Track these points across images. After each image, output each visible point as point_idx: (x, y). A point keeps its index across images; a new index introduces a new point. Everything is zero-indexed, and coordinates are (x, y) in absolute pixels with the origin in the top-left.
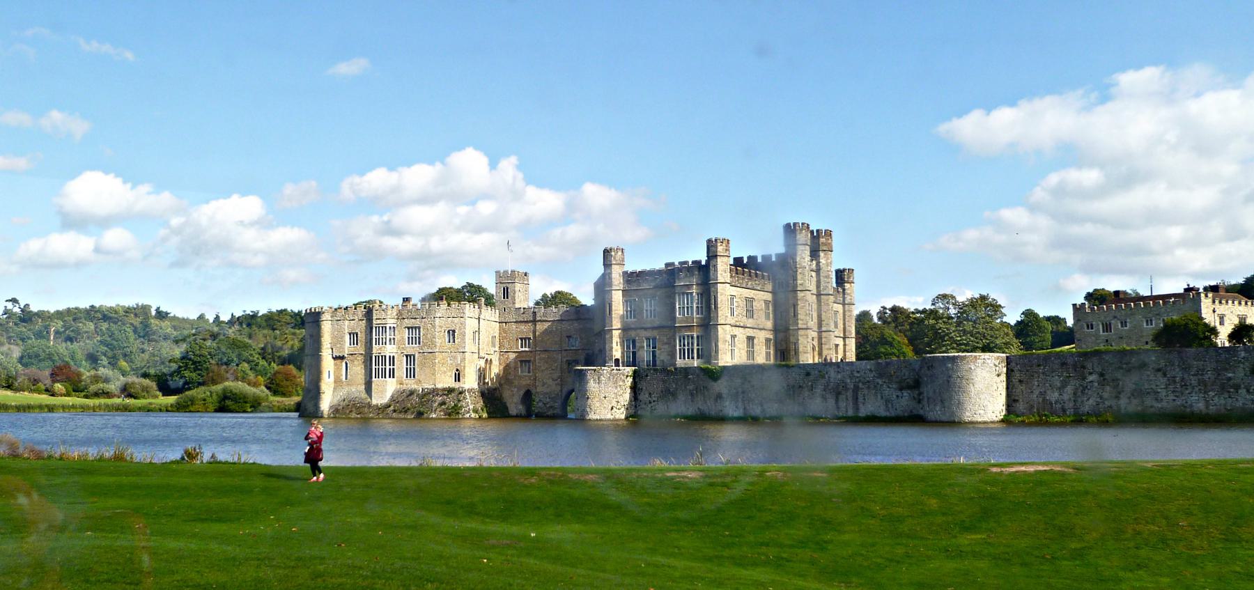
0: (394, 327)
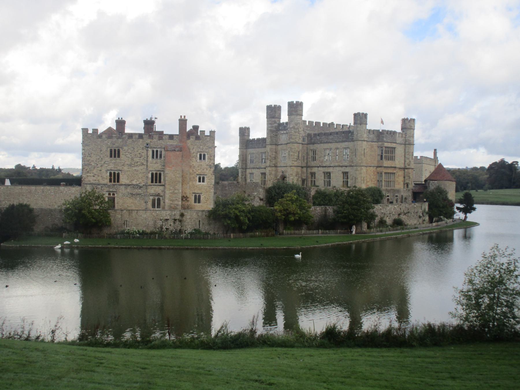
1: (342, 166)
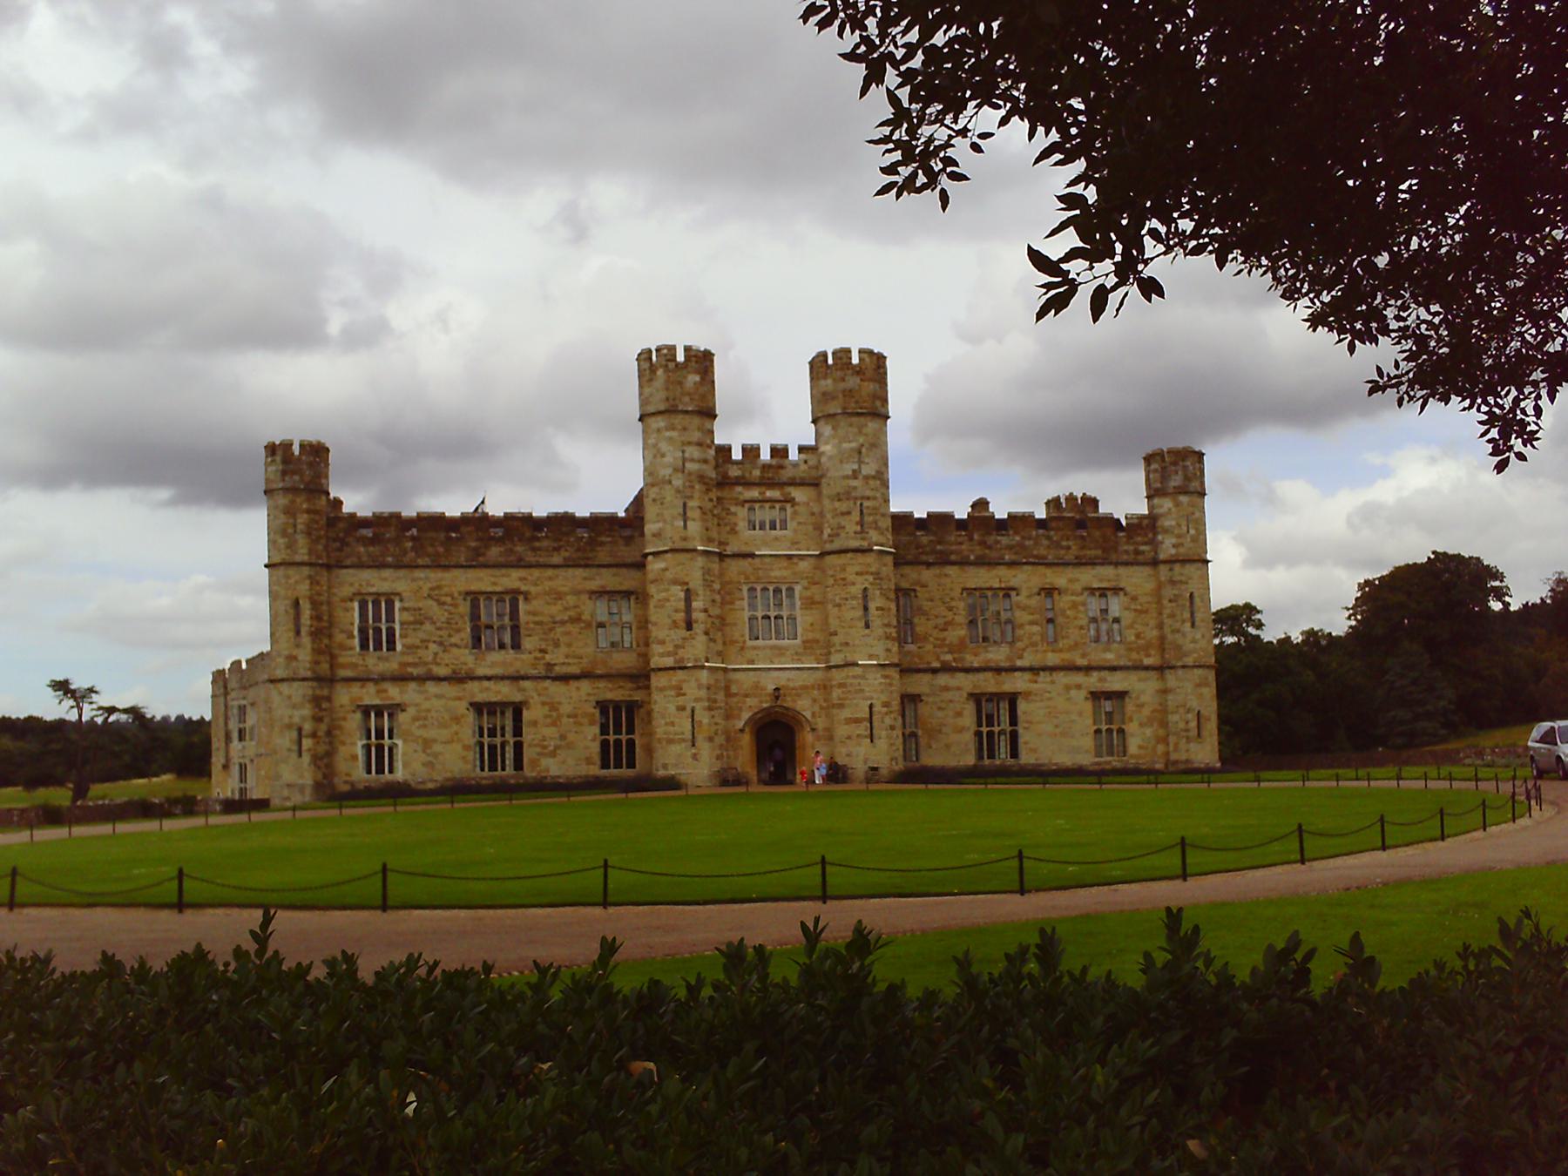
0: (245, 706)
1: (1088, 669)
